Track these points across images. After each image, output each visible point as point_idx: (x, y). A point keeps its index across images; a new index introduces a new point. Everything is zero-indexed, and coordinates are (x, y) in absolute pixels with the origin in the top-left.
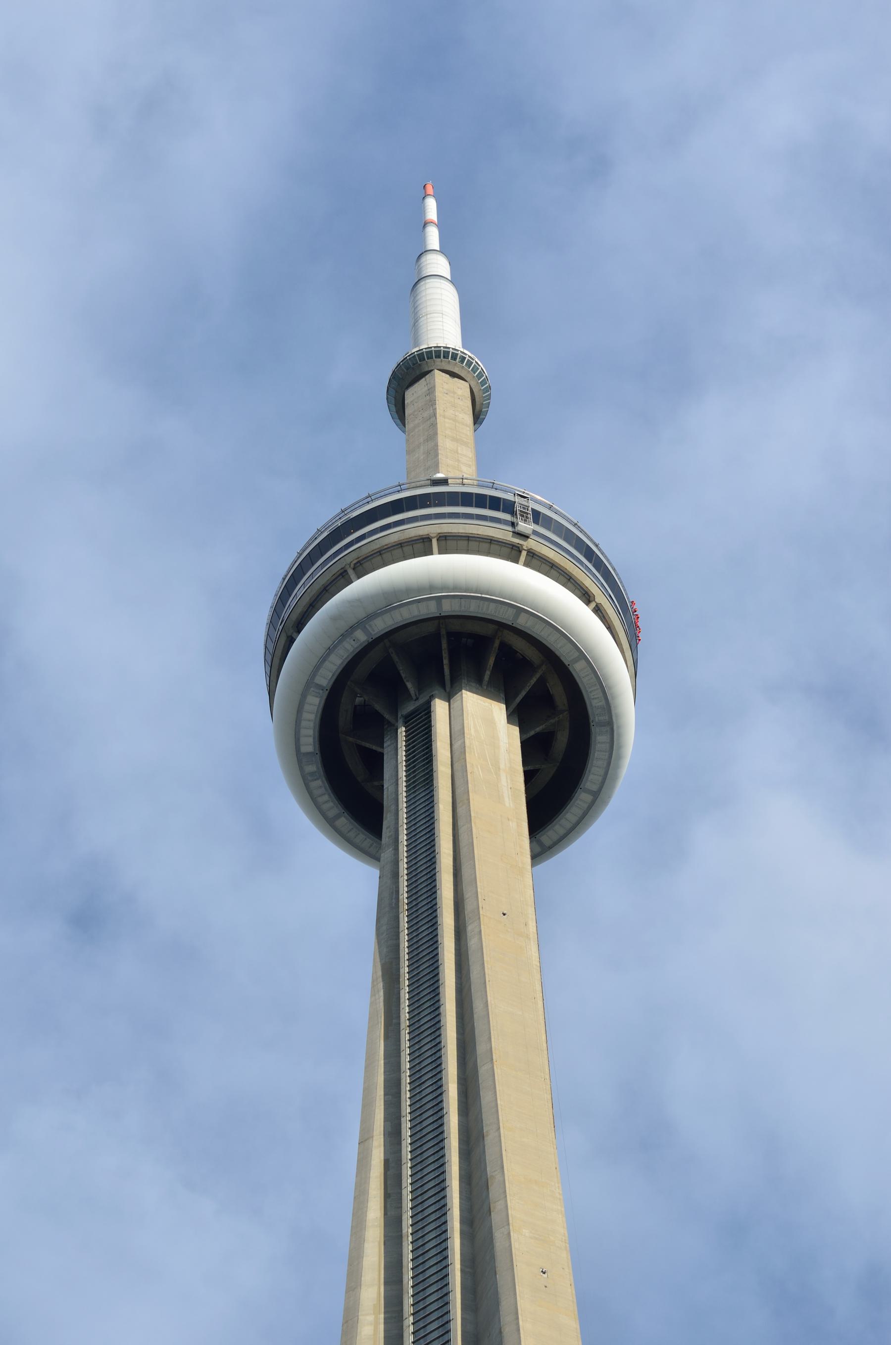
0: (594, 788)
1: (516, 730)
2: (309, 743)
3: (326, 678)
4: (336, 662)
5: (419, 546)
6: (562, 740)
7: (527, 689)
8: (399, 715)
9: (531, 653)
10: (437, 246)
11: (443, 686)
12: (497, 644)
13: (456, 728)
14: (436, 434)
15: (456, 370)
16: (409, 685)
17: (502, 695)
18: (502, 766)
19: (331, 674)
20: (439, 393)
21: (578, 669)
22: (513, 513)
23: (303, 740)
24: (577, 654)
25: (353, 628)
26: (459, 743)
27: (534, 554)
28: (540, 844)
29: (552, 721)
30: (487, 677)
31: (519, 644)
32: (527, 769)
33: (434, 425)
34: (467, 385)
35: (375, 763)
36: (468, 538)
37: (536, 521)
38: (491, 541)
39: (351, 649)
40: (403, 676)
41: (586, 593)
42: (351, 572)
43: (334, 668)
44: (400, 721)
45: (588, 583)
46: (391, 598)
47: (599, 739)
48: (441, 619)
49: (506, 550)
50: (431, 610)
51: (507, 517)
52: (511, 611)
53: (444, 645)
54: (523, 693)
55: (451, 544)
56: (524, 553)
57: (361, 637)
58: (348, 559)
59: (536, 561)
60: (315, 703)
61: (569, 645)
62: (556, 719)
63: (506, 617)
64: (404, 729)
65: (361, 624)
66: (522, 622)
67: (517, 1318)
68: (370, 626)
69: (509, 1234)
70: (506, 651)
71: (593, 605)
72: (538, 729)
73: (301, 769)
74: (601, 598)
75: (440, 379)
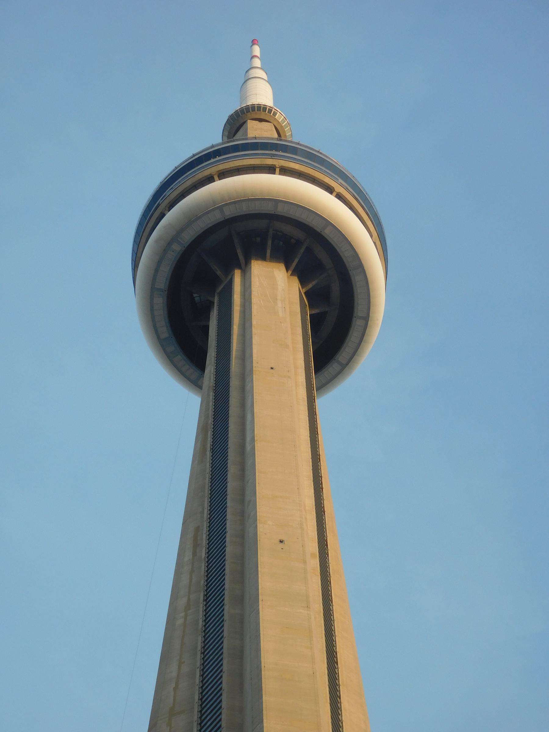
1: (295, 283)
6: (336, 289)
9: (298, 234)
10: (259, 66)
11: (240, 267)
15: (262, 117)
21: (327, 233)
25: (169, 244)
31: (287, 229)
45: (327, 180)
46: (191, 218)
57: (177, 248)
63: (268, 209)
66: (281, 210)
71: (335, 194)
73: (165, 351)
74: (339, 189)
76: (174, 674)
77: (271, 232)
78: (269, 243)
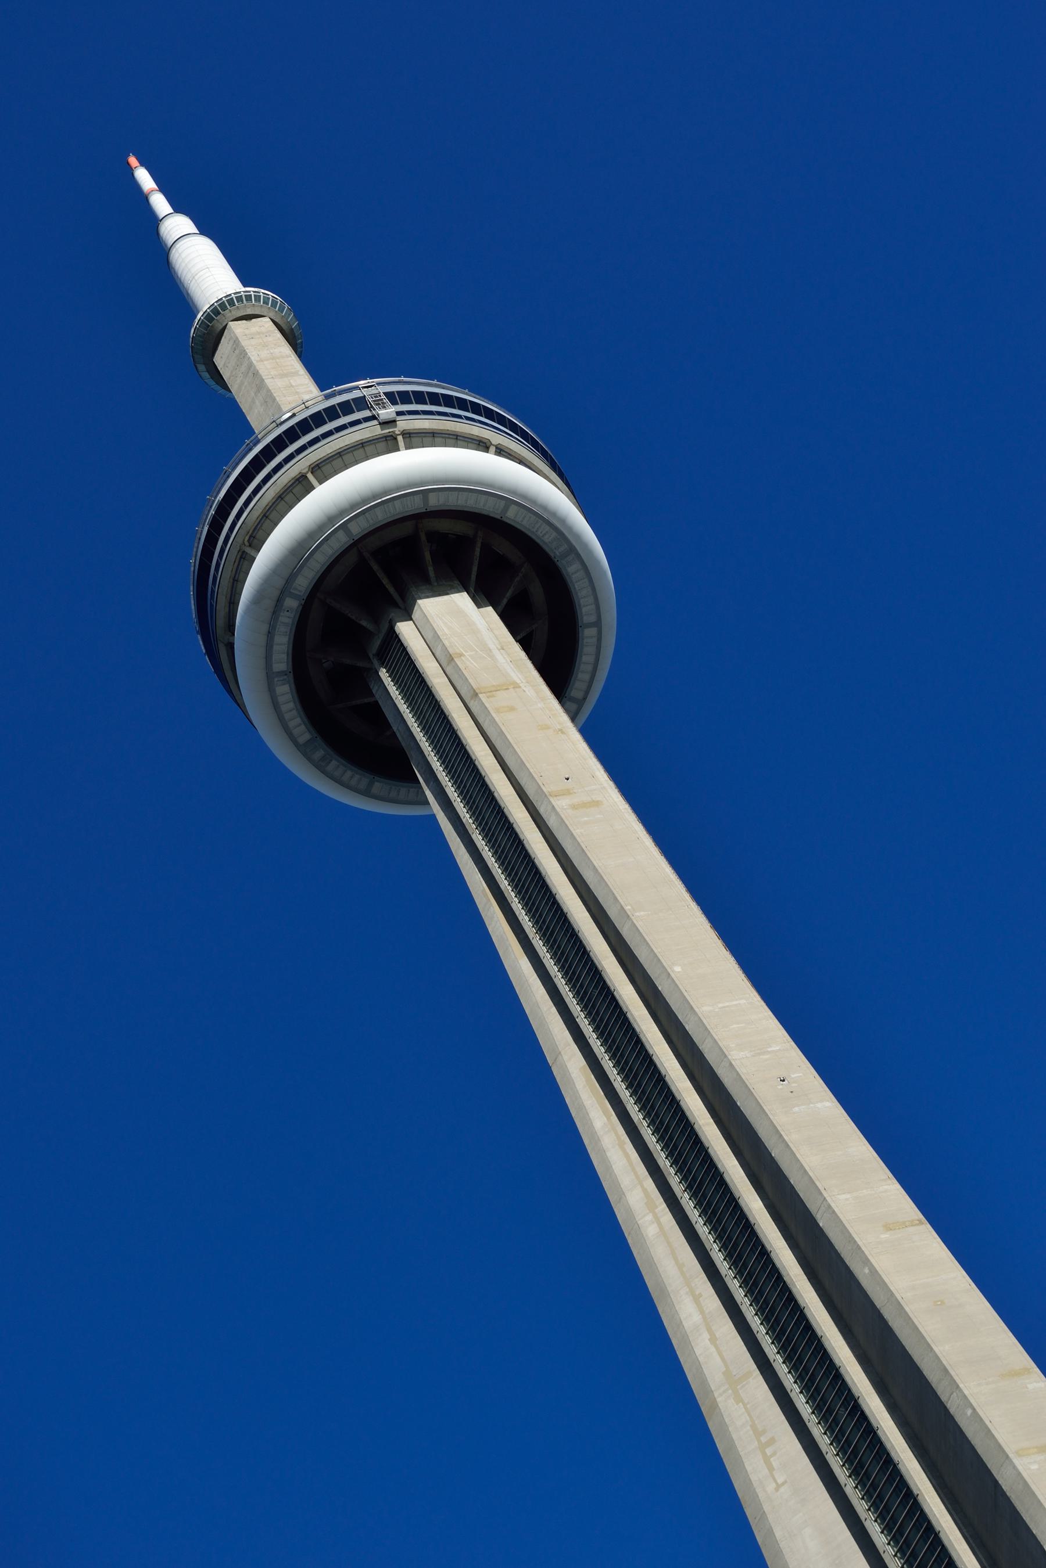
0: (593, 619)
3: (282, 662)
4: (283, 642)
5: (298, 489)
6: (537, 593)
7: (476, 563)
8: (371, 656)
10: (168, 209)
12: (423, 537)
13: (429, 636)
14: (263, 380)
15: (249, 312)
16: (364, 623)
17: (457, 582)
18: (492, 646)
19: (284, 656)
20: (244, 343)
21: (512, 516)
22: (369, 408)
23: (296, 732)
24: (503, 503)
25: (279, 601)
26: (439, 647)
27: (410, 433)
28: (573, 700)
29: (517, 579)
31: (444, 526)
32: (519, 638)
33: (256, 374)
34: (267, 319)
35: (377, 715)
36: (340, 454)
37: (394, 402)
38: (362, 444)
39: (289, 621)
40: (353, 617)
41: (480, 441)
42: (248, 550)
43: (284, 648)
44: (376, 662)
46: (298, 553)
47: (572, 571)
48: (356, 544)
49: (381, 445)
50: (342, 541)
51: (366, 413)
52: (418, 499)
53: (375, 567)
54: (475, 569)
55: (326, 469)
56: (400, 438)
57: (292, 604)
58: (240, 540)
59: (415, 439)
60: (285, 691)
61: (492, 498)
62: (521, 575)
63: (416, 506)
64: (384, 670)
65: (284, 592)
66: (434, 502)
67: (781, 1136)
68: (295, 589)
69: (731, 1064)
70: (434, 537)
71: (492, 449)
72: (509, 594)
73: (310, 760)
75: (238, 328)
76: (697, 1318)
77: (423, 537)
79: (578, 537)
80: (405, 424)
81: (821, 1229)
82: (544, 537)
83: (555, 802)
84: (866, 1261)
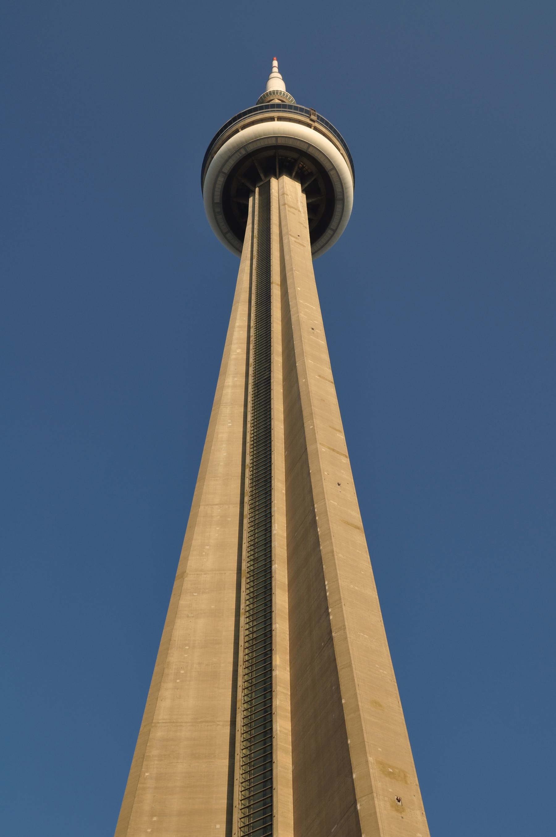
0: (334, 228)
1: (305, 196)
2: (218, 199)
3: (227, 169)
13: (280, 187)
18: (299, 199)
21: (332, 173)
30: (294, 174)
39: (238, 157)
47: (338, 206)
52: (306, 146)
57: (243, 152)
60: (221, 180)
63: (304, 147)
78: (296, 168)
79: (348, 197)
80: (316, 125)
81: (296, 366)
82: (337, 189)
83: (291, 238)
84: (306, 378)
